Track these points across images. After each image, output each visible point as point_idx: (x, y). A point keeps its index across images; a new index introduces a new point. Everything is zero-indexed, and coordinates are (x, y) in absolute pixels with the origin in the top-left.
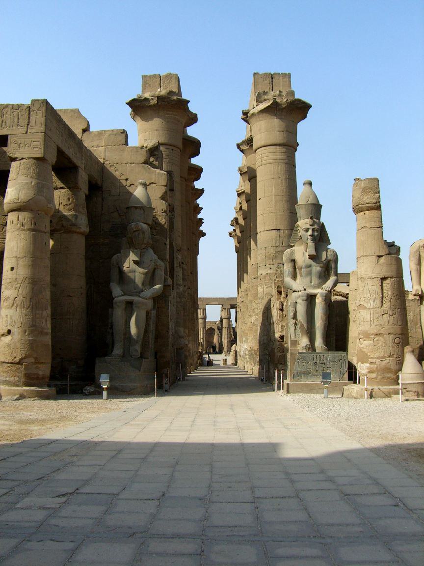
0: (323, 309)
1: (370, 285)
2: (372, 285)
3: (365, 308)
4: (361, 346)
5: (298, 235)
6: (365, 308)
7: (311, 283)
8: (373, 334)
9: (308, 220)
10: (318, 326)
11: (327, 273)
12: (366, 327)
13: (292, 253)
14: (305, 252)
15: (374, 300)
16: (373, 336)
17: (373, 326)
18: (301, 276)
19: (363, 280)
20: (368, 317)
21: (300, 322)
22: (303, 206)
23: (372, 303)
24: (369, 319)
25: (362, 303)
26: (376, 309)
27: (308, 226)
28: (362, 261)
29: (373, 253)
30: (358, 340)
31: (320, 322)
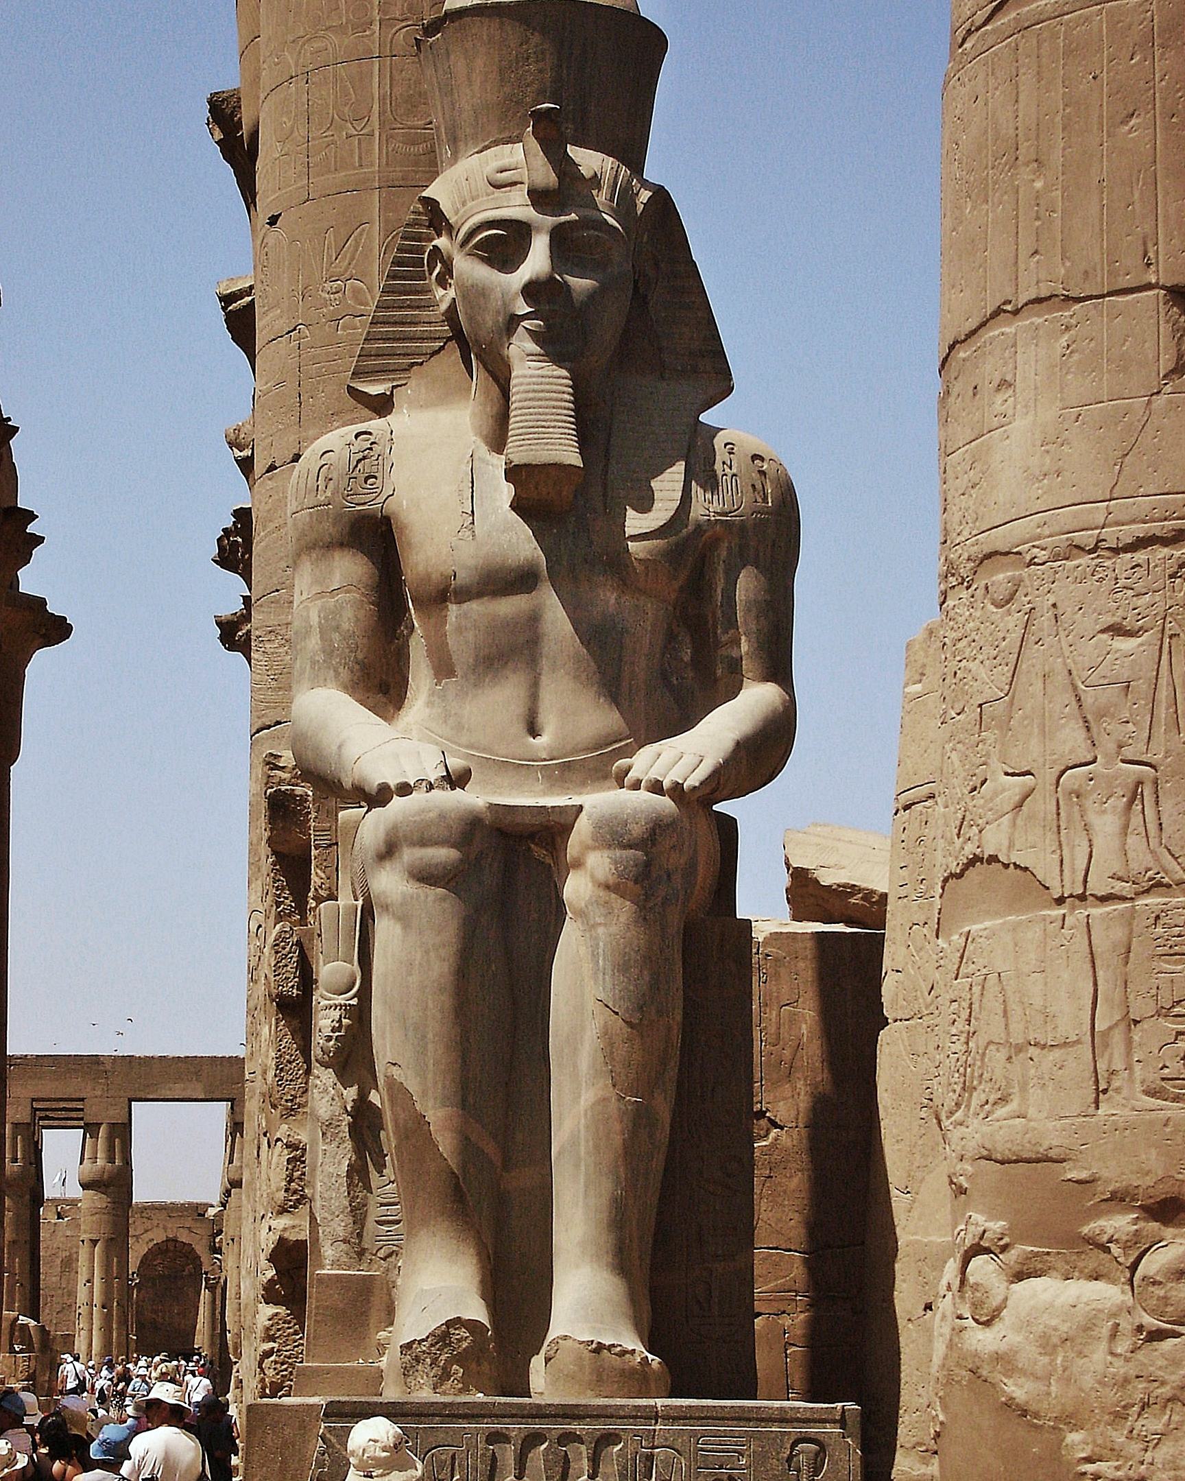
0: (622, 967)
1: (1089, 623)
2: (1116, 630)
3: (1026, 885)
4: (982, 1340)
5: (432, 305)
6: (1026, 885)
7: (533, 730)
8: (1119, 1199)
9: (513, 154)
10: (574, 1141)
11: (687, 655)
12: (1039, 1115)
13: (367, 465)
14: (483, 450)
15: (1134, 796)
16: (1120, 1224)
17: (1128, 1103)
18: (443, 668)
19: (1000, 578)
20: (1063, 998)
21: (397, 1091)
22: (482, 29)
23: (1106, 824)
24: (1070, 1020)
25: (994, 841)
26: (1153, 901)
27: (517, 206)
28: (991, 369)
29: (1132, 260)
30: (952, 1266)
31: (588, 1097)
